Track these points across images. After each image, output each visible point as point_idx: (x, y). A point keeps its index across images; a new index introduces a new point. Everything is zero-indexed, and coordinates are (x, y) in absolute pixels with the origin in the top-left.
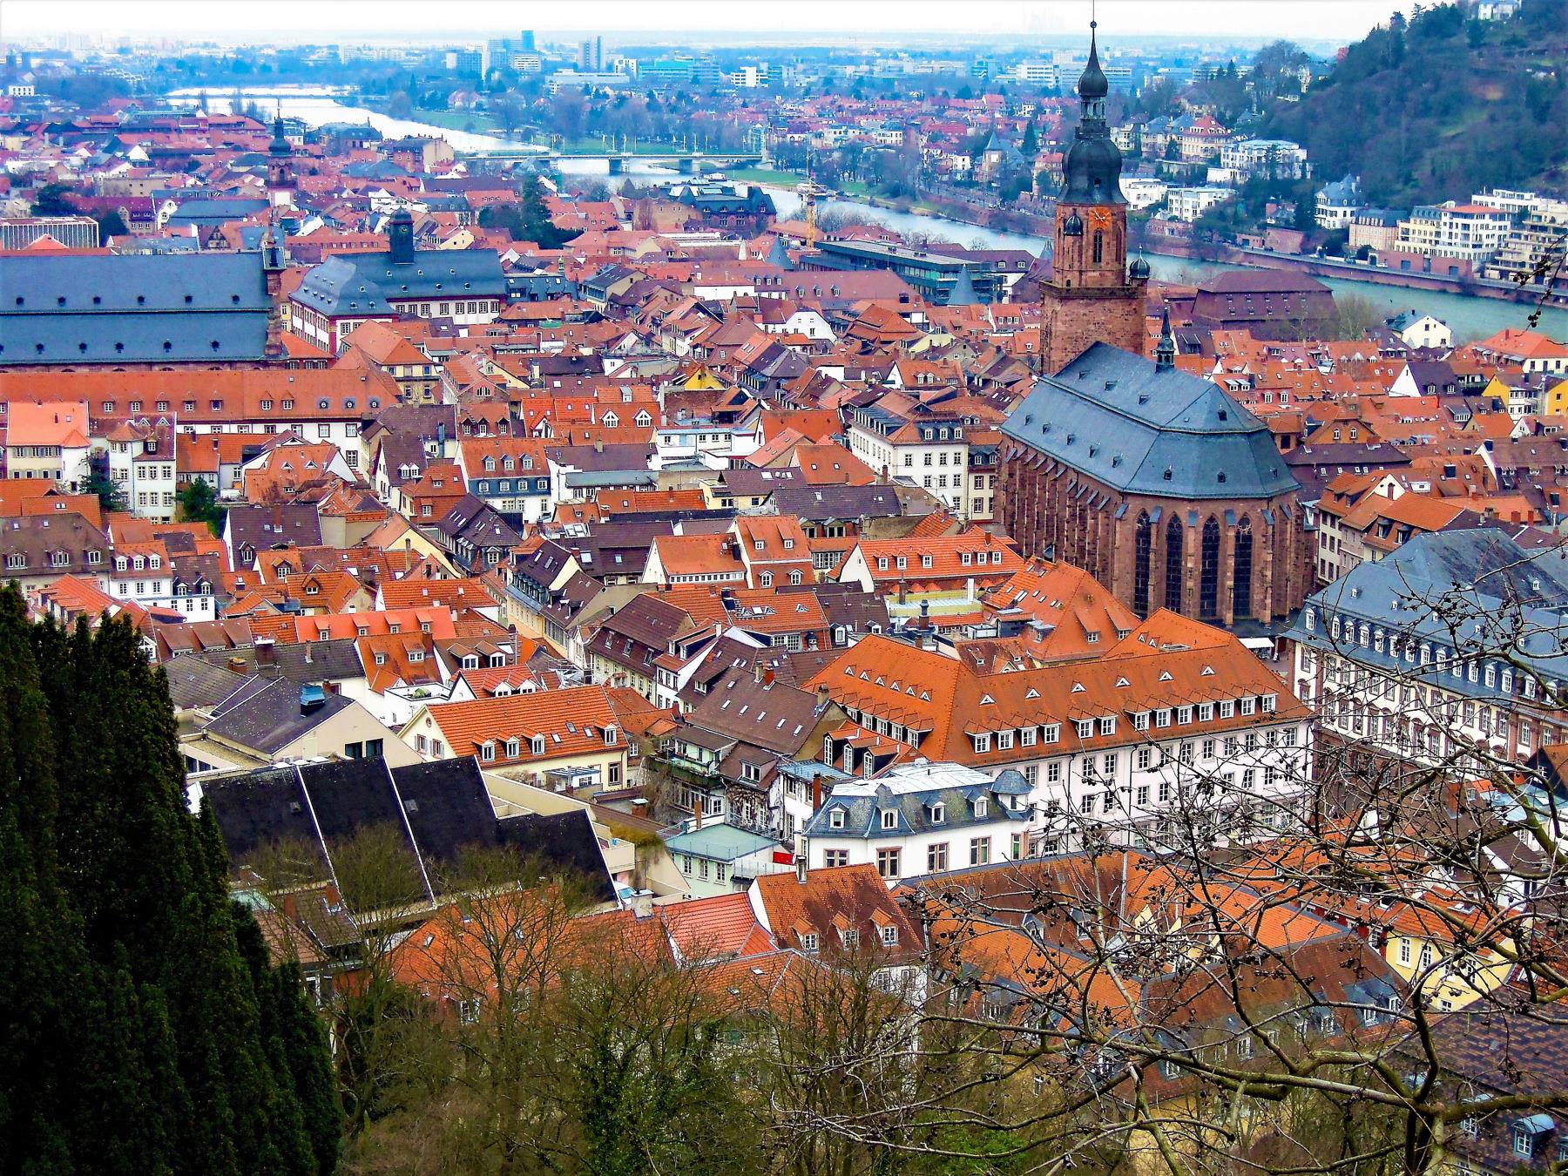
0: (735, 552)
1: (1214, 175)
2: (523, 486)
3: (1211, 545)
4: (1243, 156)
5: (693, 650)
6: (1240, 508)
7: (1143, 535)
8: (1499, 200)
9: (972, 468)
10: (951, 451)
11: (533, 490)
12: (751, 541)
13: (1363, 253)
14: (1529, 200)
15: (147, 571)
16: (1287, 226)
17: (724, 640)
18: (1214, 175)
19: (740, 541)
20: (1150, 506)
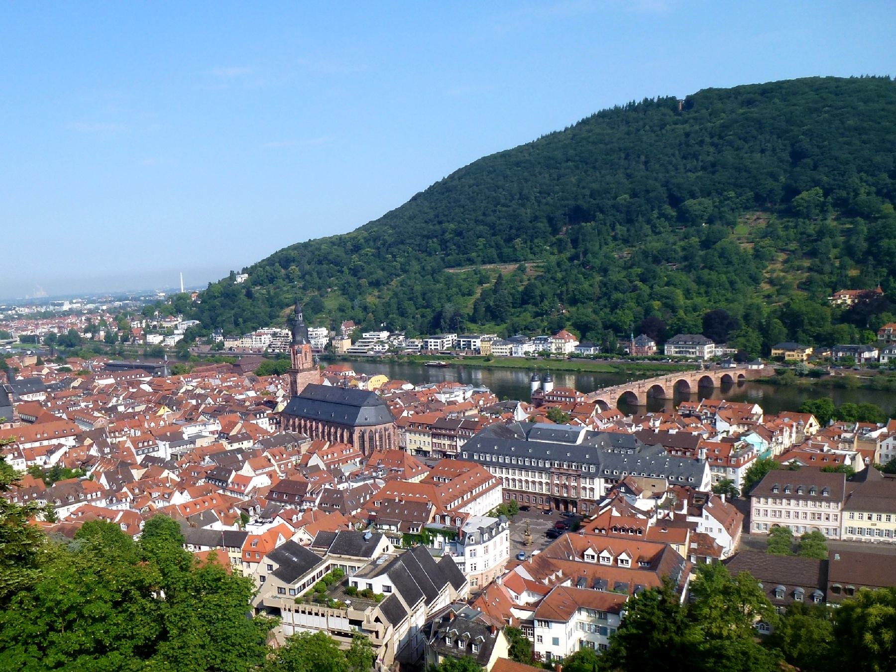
0: (269, 460)
1: (176, 332)
2: (151, 450)
3: (381, 438)
4: (181, 325)
5: (318, 494)
6: (387, 425)
7: (362, 437)
8: (265, 330)
9: (270, 424)
10: (264, 420)
11: (154, 451)
12: (274, 456)
13: (231, 349)
14: (274, 330)
15: (98, 499)
16: (204, 343)
17: (326, 490)
18: (176, 332)
19: (270, 457)
20: (363, 428)
